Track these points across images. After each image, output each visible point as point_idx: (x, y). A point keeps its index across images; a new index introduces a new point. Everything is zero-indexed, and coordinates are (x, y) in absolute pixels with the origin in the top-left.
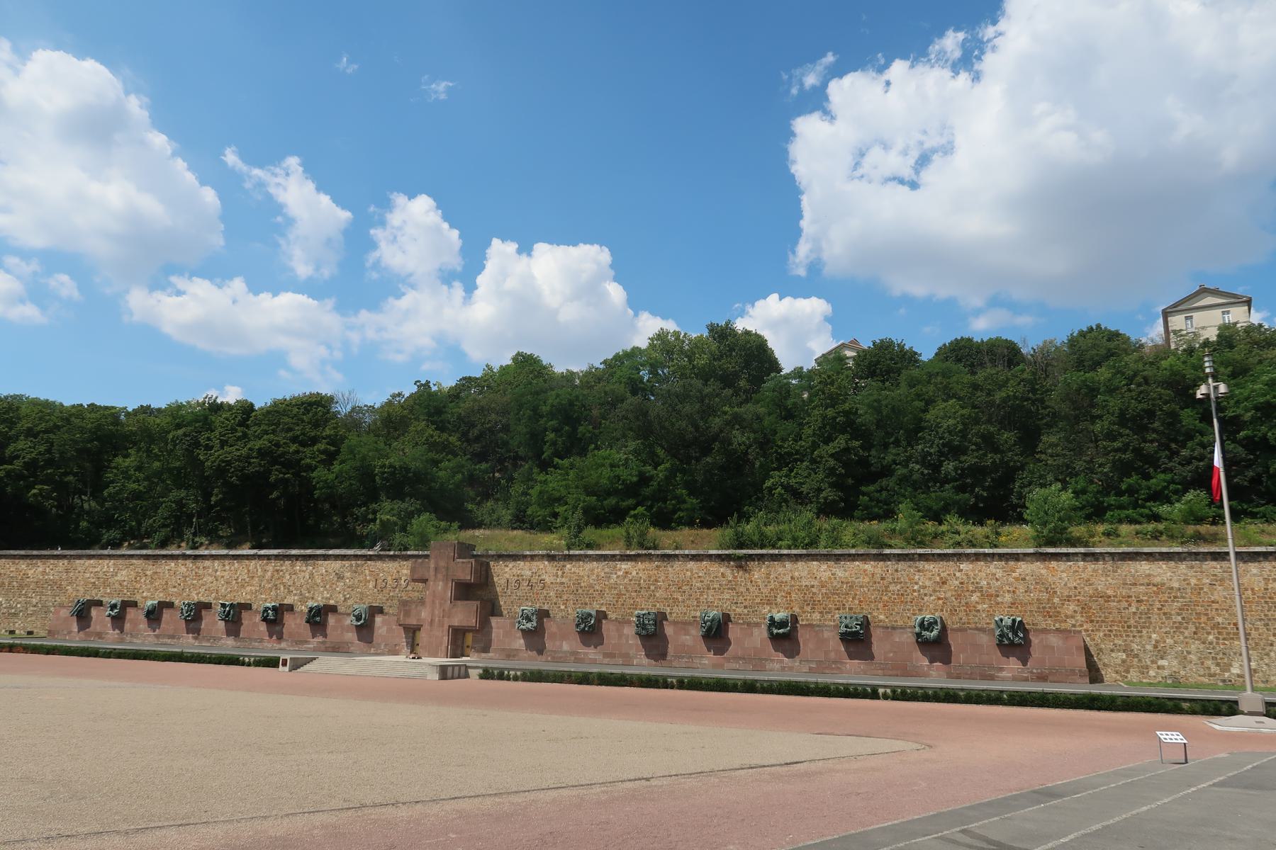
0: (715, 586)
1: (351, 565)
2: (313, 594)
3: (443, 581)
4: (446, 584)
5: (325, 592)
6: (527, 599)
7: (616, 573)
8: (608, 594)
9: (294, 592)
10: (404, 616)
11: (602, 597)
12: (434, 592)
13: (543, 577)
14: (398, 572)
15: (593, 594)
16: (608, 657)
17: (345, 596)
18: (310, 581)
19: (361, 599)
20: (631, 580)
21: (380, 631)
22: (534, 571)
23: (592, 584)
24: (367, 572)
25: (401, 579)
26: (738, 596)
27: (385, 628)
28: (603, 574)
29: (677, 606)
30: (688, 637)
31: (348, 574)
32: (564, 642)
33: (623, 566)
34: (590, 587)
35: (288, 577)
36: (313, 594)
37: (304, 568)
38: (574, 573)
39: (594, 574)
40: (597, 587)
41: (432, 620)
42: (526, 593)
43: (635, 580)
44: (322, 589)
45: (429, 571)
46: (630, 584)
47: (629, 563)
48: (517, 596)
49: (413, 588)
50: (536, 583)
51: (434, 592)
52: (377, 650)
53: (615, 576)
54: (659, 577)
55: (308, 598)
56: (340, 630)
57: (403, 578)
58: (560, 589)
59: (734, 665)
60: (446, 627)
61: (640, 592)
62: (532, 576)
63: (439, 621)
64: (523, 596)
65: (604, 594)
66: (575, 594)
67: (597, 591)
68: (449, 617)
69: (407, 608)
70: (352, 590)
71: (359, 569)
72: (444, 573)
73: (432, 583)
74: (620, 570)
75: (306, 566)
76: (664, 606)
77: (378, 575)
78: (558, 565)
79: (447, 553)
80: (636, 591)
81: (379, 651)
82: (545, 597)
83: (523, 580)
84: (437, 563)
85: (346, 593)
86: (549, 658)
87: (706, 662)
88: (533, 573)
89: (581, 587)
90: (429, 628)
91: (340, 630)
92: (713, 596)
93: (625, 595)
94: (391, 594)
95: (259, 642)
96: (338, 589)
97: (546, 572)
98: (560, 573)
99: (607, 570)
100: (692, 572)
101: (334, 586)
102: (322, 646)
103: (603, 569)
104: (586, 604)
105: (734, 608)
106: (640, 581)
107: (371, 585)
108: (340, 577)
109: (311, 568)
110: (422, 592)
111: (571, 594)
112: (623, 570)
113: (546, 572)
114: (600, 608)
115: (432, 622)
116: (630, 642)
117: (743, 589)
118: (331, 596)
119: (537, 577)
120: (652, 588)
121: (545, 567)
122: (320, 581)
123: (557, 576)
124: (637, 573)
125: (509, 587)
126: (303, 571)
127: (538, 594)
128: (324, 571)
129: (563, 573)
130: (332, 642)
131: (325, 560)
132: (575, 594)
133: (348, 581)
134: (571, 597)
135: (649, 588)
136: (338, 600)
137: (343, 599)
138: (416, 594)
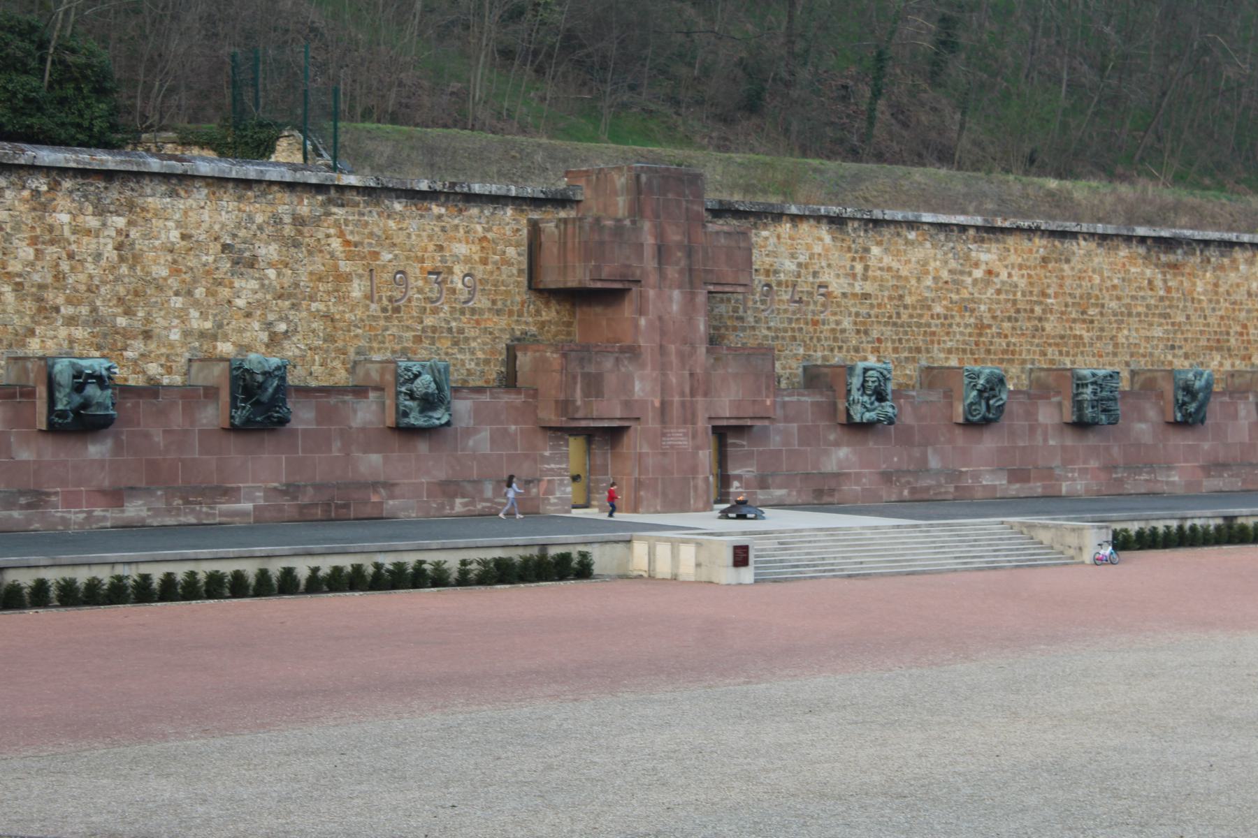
0: (1140, 309)
1: (277, 221)
2: (147, 320)
3: (680, 287)
4: (690, 298)
5: (194, 313)
6: (794, 338)
7: (970, 274)
8: (958, 325)
9: (67, 310)
10: (586, 394)
11: (948, 334)
12: (660, 318)
13: (824, 278)
14: (440, 248)
15: (929, 325)
16: (1017, 481)
17: (268, 325)
18: (124, 269)
19: (330, 339)
20: (999, 292)
21: (471, 443)
22: (802, 259)
23: (926, 298)
24: (336, 244)
25: (450, 271)
26: (1175, 332)
27: (485, 434)
28: (945, 275)
29: (1082, 353)
30: (1143, 426)
31: (269, 251)
32: (930, 450)
33: (984, 257)
34: (922, 307)
35: (28, 253)
36: (147, 320)
37: (93, 222)
38: (889, 269)
39: (927, 273)
40: (938, 309)
41: (663, 403)
42: (790, 321)
43: (1007, 292)
44: (177, 302)
45: (640, 256)
46: (998, 302)
47: (994, 247)
48: (769, 328)
49: (494, 302)
50: (810, 294)
51: (660, 318)
52: (472, 503)
53: (969, 280)
54: (1049, 286)
55: (126, 334)
56: (336, 445)
57: (458, 269)
58: (864, 311)
59: (1216, 483)
60: (702, 424)
61: (1016, 320)
62: (799, 276)
63: (683, 404)
64: (785, 331)
65: (950, 325)
66: (895, 324)
67: (938, 316)
68: (706, 394)
69: (592, 369)
70: (293, 306)
71: (305, 230)
72: (683, 263)
73: (652, 293)
74: (977, 265)
75: (100, 211)
76: (1061, 353)
77: (376, 255)
78: (853, 246)
79: (684, 203)
80: (1009, 319)
81: (479, 507)
82: (833, 330)
83: (779, 284)
84: (660, 235)
85: (271, 317)
86: (906, 493)
87: (1176, 479)
88: (799, 265)
89: (906, 307)
90: (658, 426)
91: (336, 445)
92: (1137, 330)
93: (989, 326)
94: (429, 321)
95: (29, 506)
96: (240, 302)
97: (829, 266)
98: (859, 267)
99: (953, 264)
100: (1101, 274)
101: (225, 292)
102: (286, 502)
103: (946, 262)
104: (918, 350)
105: (1170, 357)
106: (1015, 294)
107: (357, 290)
108: (244, 263)
109: (120, 222)
110: (520, 314)
111: (886, 324)
112: (983, 267)
113: (829, 266)
114: (947, 359)
115: (664, 407)
116: (1051, 442)
117: (1181, 318)
118: (220, 326)
119: (811, 279)
120: (1038, 310)
121: (827, 250)
122: (164, 272)
123: (854, 276)
124: (1010, 275)
125: (750, 304)
126: (88, 232)
127: (815, 323)
128: (175, 235)
129: (866, 268)
130: (318, 487)
131: (173, 194)
132: (895, 324)
133: (271, 273)
134: (888, 331)
135: (1032, 311)
136: (247, 338)
137: (264, 336)
138: (503, 322)
